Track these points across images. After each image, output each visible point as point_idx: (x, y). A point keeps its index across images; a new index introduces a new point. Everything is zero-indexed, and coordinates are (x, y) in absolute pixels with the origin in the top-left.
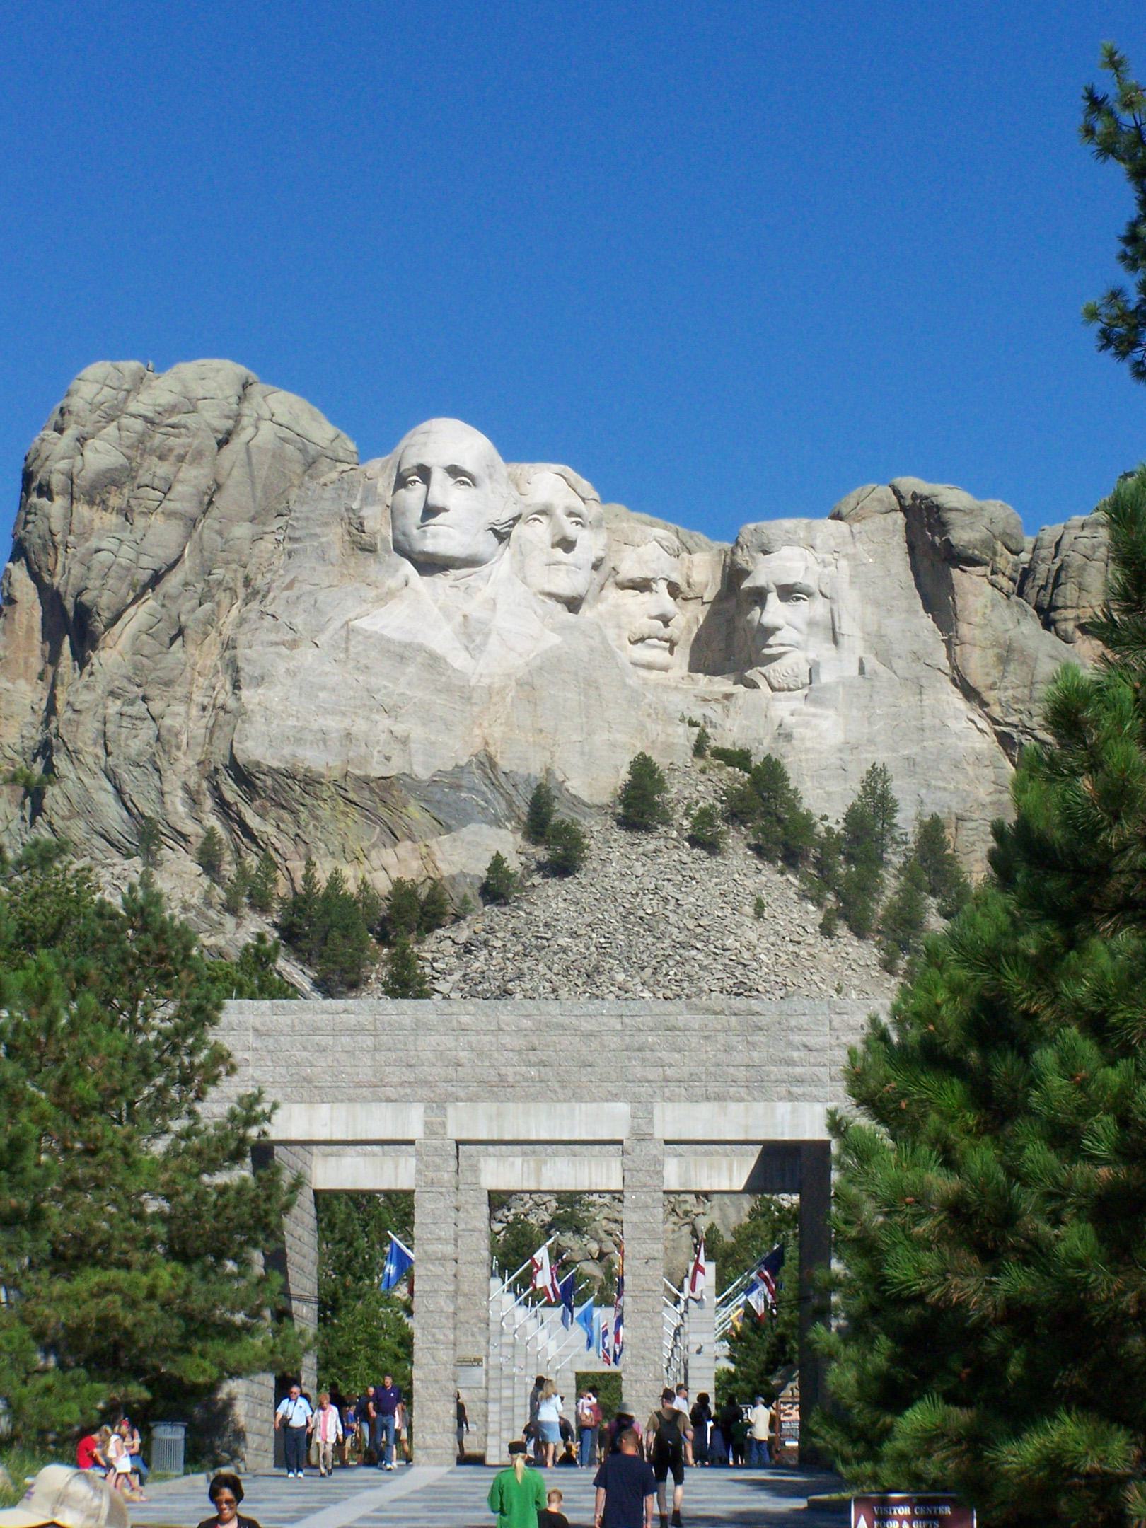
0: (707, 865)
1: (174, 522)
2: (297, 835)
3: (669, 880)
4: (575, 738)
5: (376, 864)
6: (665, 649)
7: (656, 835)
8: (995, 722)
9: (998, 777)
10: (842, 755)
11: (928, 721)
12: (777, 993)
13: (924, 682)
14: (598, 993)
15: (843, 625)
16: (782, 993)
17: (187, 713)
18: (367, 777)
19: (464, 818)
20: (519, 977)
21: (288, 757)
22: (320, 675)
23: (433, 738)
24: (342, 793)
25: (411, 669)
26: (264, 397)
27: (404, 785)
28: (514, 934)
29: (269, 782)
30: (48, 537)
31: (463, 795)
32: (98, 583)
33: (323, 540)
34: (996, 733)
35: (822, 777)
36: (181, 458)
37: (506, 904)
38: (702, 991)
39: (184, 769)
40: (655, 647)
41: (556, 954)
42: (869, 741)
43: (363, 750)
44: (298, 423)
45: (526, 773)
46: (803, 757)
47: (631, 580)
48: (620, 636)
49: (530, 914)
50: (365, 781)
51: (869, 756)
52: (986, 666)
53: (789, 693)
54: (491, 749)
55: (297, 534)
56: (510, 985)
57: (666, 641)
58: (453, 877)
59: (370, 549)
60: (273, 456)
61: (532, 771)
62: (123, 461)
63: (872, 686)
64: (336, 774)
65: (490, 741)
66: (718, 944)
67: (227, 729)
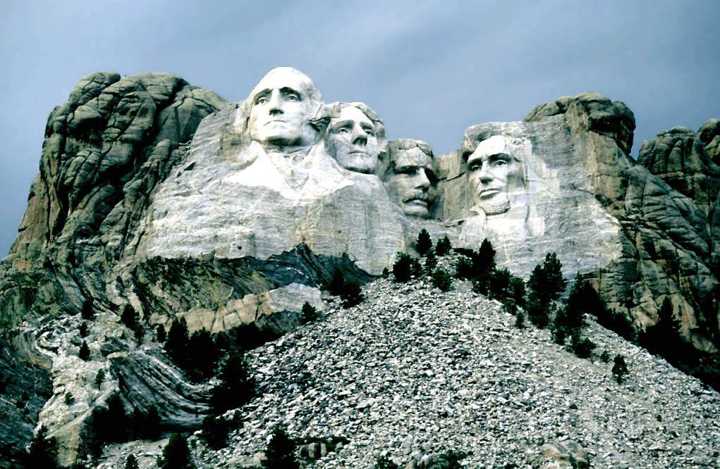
0: (442, 295)
1: (126, 145)
2: (183, 297)
3: (416, 303)
4: (360, 238)
5: (230, 309)
6: (424, 206)
7: (410, 283)
8: (623, 219)
9: (625, 248)
10: (528, 243)
11: (580, 221)
12: (484, 356)
13: (577, 199)
14: (364, 363)
15: (528, 175)
16: (487, 355)
17: (123, 239)
18: (226, 259)
19: (287, 280)
20: (314, 357)
21: (178, 253)
22: (201, 207)
23: (269, 236)
24: (210, 269)
25: (259, 201)
26: (191, 90)
27: (250, 263)
28: (313, 337)
29: (166, 268)
30: (51, 156)
31: (289, 268)
32: (74, 173)
33: (211, 143)
34: (622, 225)
35: (516, 256)
36: (134, 114)
37: (312, 324)
38: (431, 356)
39: (119, 269)
40: (418, 204)
41: (338, 345)
42: (545, 233)
43: (225, 245)
44: (209, 100)
45: (329, 255)
46: (505, 246)
47: (404, 167)
48: (397, 200)
49: (325, 327)
50: (224, 262)
51: (545, 242)
52: (616, 187)
53: (496, 216)
54: (307, 242)
55: (197, 143)
56: (307, 363)
57: (425, 201)
58: (279, 314)
59: (234, 144)
60: (192, 114)
61: (333, 255)
62: (98, 115)
63: (547, 204)
64: (207, 259)
65: (307, 238)
66: (445, 332)
67: (144, 244)
